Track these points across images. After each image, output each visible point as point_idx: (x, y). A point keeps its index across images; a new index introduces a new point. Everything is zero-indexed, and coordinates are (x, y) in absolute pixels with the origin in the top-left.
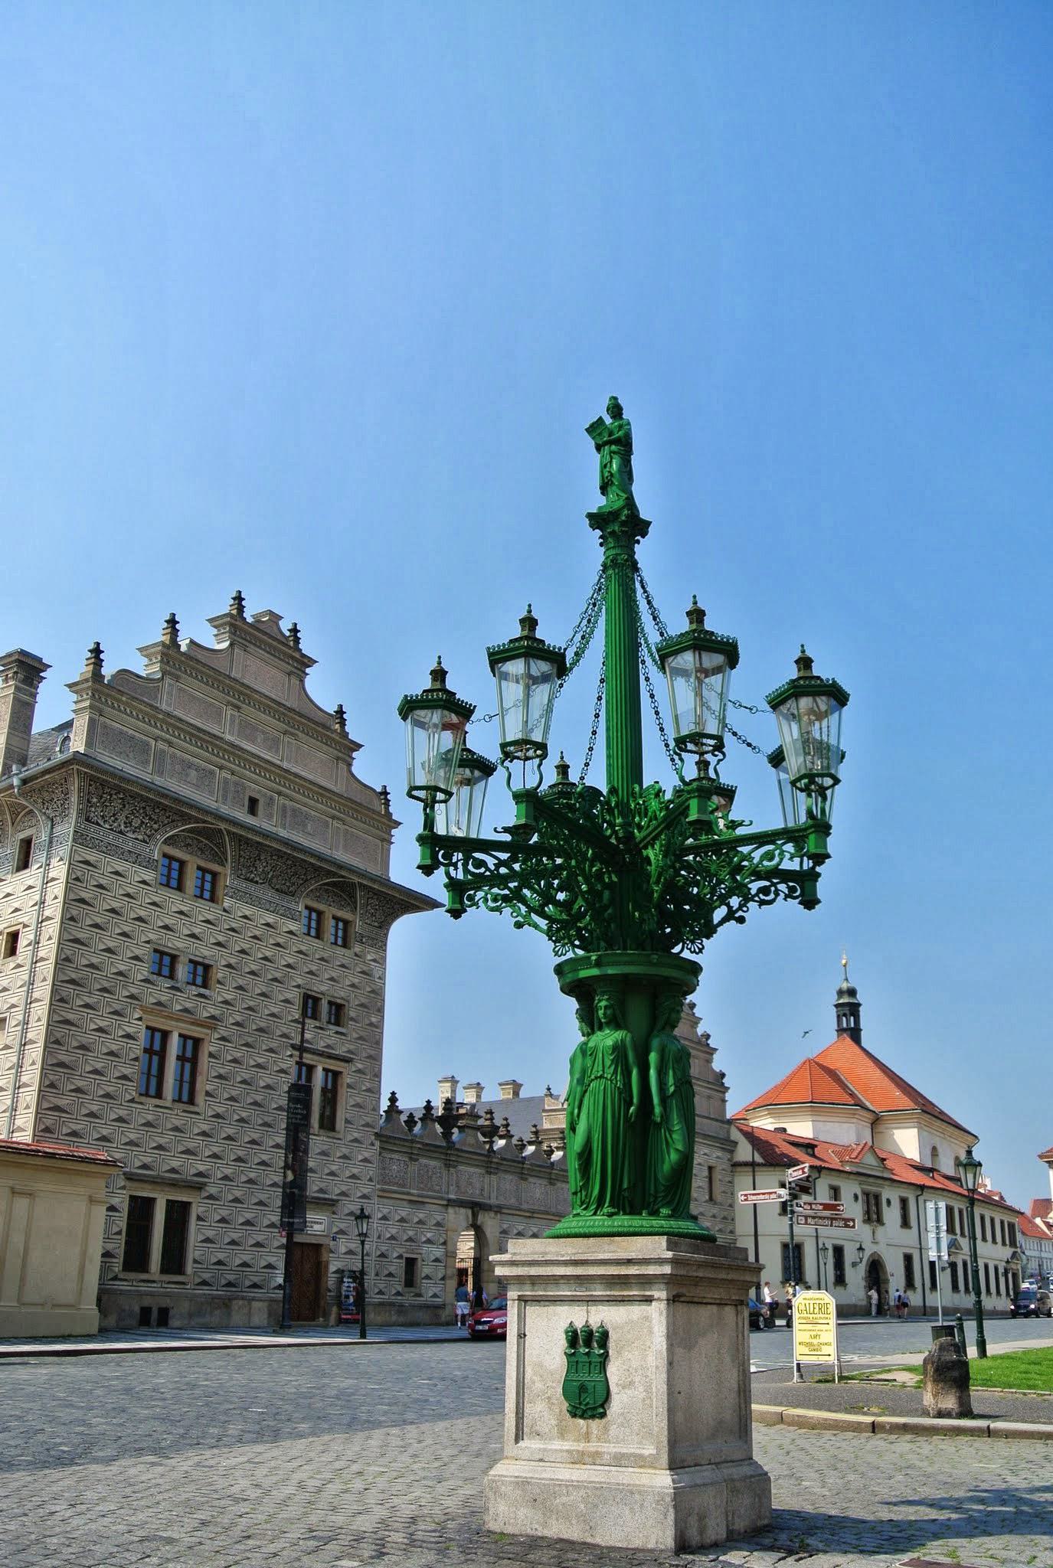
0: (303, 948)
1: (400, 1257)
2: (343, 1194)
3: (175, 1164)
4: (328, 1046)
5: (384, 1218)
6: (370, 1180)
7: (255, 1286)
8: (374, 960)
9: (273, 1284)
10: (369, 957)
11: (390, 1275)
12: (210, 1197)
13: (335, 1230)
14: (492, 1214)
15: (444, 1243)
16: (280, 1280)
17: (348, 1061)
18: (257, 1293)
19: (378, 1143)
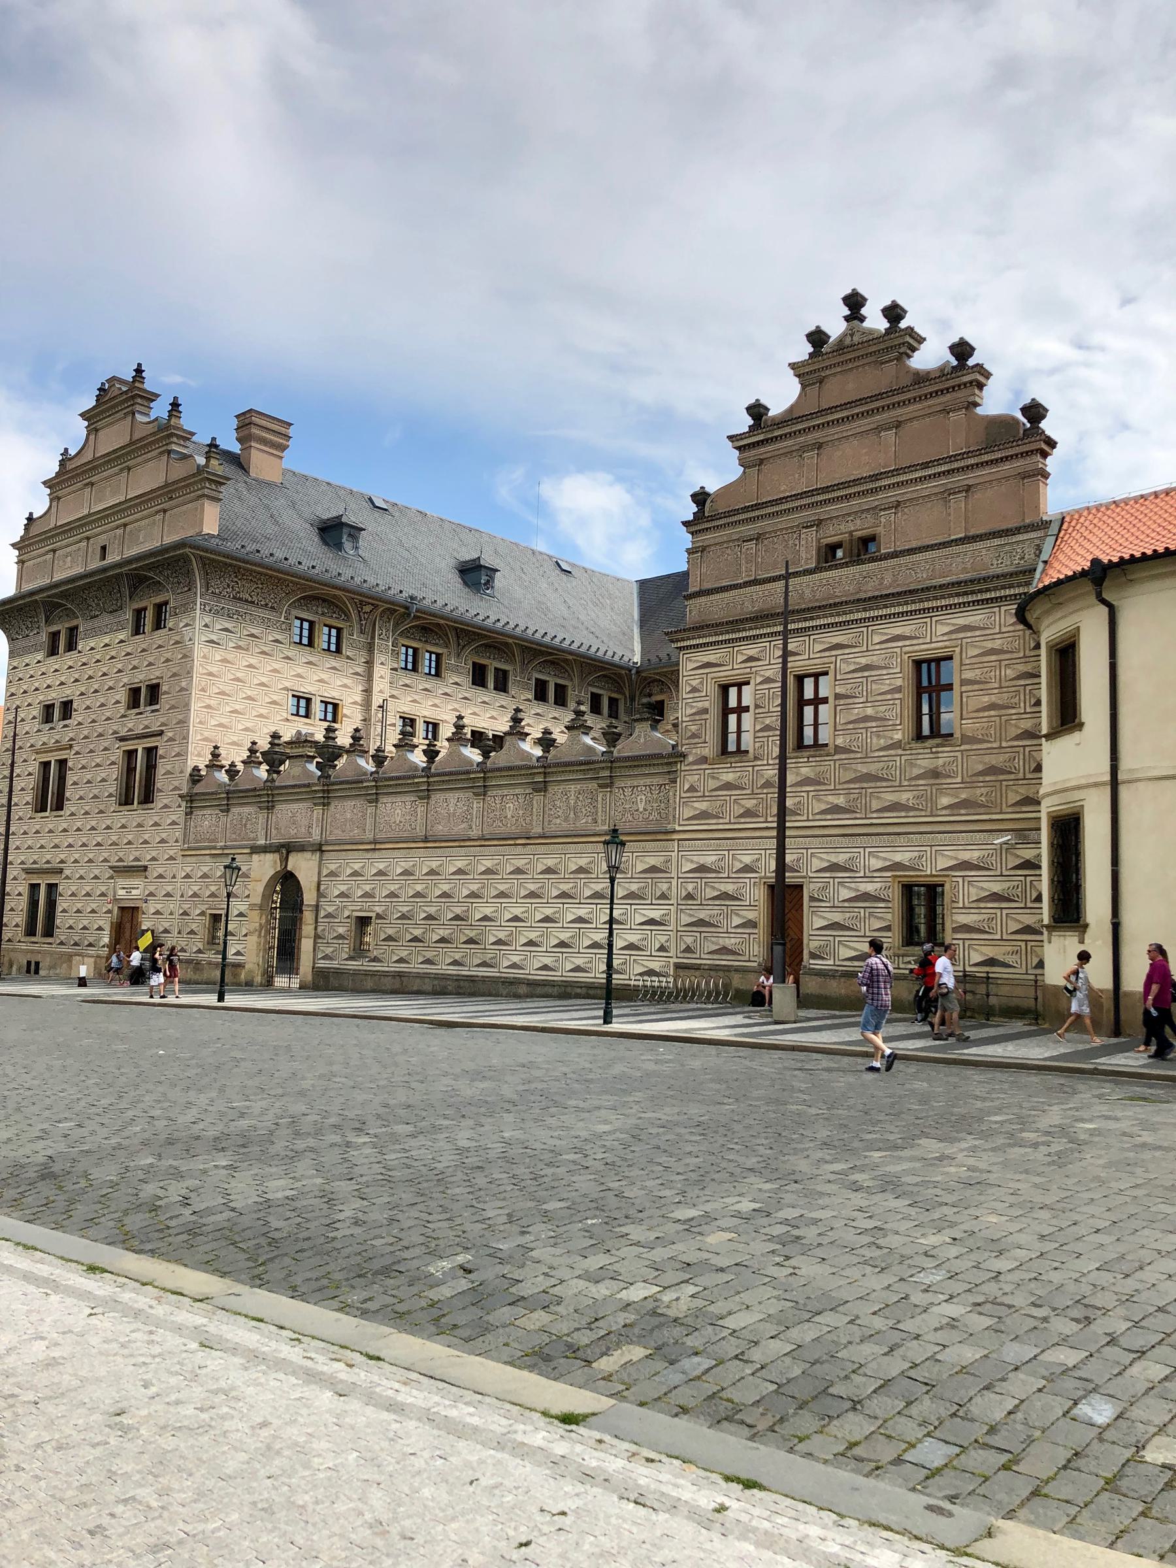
0: (129, 650)
1: (203, 914)
2: (154, 859)
3: (48, 857)
4: (146, 727)
5: (188, 876)
6: (177, 841)
7: (90, 945)
8: (187, 625)
9: (102, 944)
10: (182, 625)
11: (192, 932)
12: (67, 878)
13: (147, 893)
14: (308, 855)
15: (248, 896)
16: (106, 940)
17: (161, 733)
18: (92, 951)
19: (184, 804)
